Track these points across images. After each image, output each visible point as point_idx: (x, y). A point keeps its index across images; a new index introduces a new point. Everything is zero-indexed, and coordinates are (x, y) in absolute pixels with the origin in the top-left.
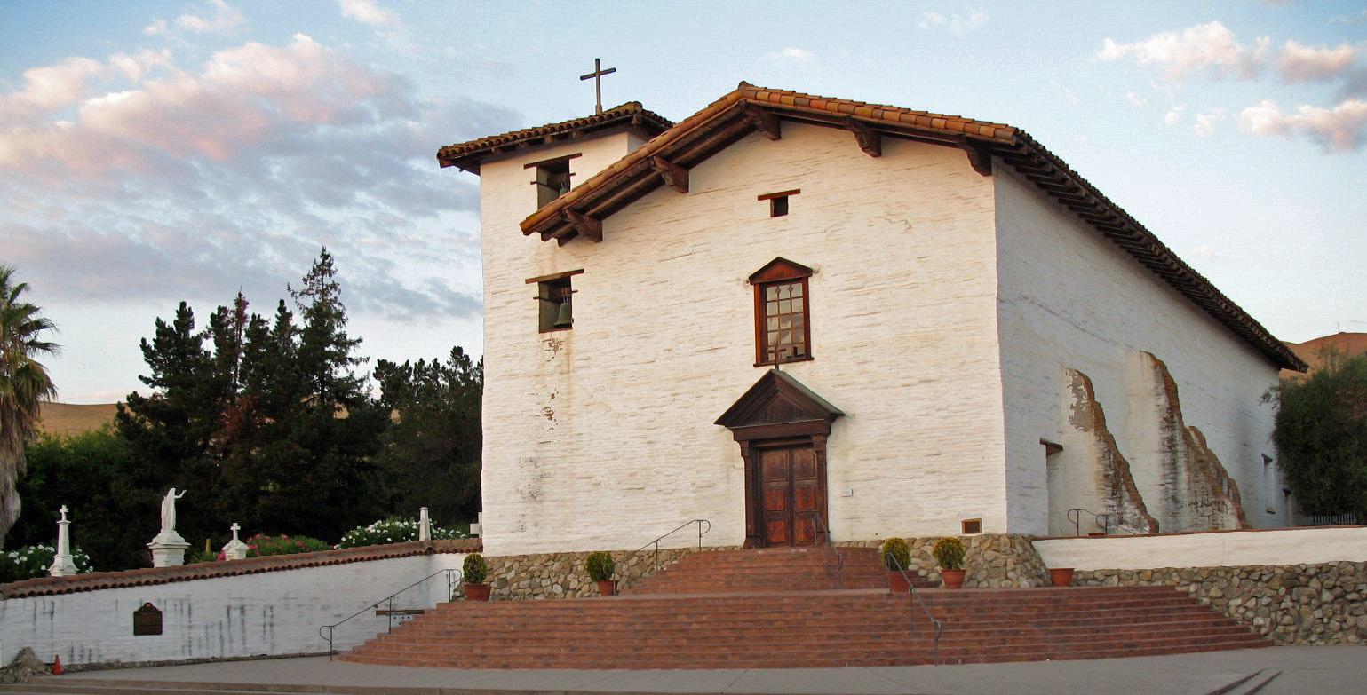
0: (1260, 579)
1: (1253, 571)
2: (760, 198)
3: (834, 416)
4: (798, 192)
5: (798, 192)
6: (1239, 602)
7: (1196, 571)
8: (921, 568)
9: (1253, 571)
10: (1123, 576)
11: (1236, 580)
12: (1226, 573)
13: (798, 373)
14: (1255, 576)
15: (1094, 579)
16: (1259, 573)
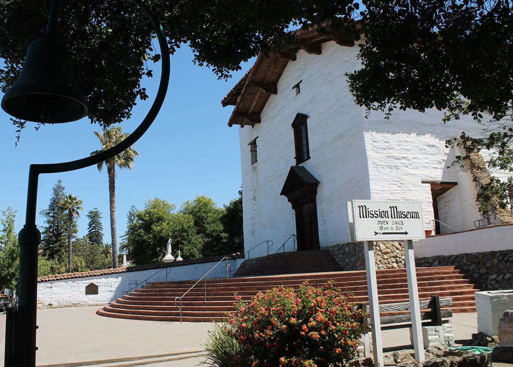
0: (509, 259)
1: (507, 254)
2: (293, 88)
3: (319, 183)
4: (301, 81)
5: (301, 81)
6: (494, 276)
7: (477, 255)
8: (341, 260)
9: (507, 254)
10: (441, 260)
11: (495, 261)
12: (493, 256)
13: (307, 165)
14: (506, 258)
15: (428, 262)
16: (509, 255)
